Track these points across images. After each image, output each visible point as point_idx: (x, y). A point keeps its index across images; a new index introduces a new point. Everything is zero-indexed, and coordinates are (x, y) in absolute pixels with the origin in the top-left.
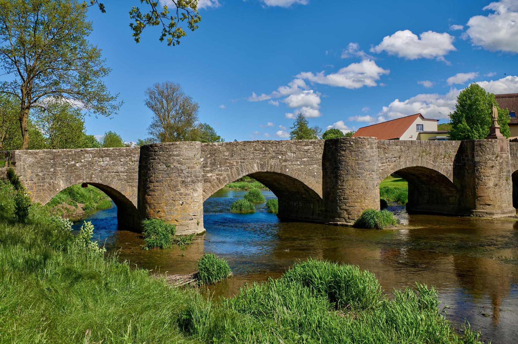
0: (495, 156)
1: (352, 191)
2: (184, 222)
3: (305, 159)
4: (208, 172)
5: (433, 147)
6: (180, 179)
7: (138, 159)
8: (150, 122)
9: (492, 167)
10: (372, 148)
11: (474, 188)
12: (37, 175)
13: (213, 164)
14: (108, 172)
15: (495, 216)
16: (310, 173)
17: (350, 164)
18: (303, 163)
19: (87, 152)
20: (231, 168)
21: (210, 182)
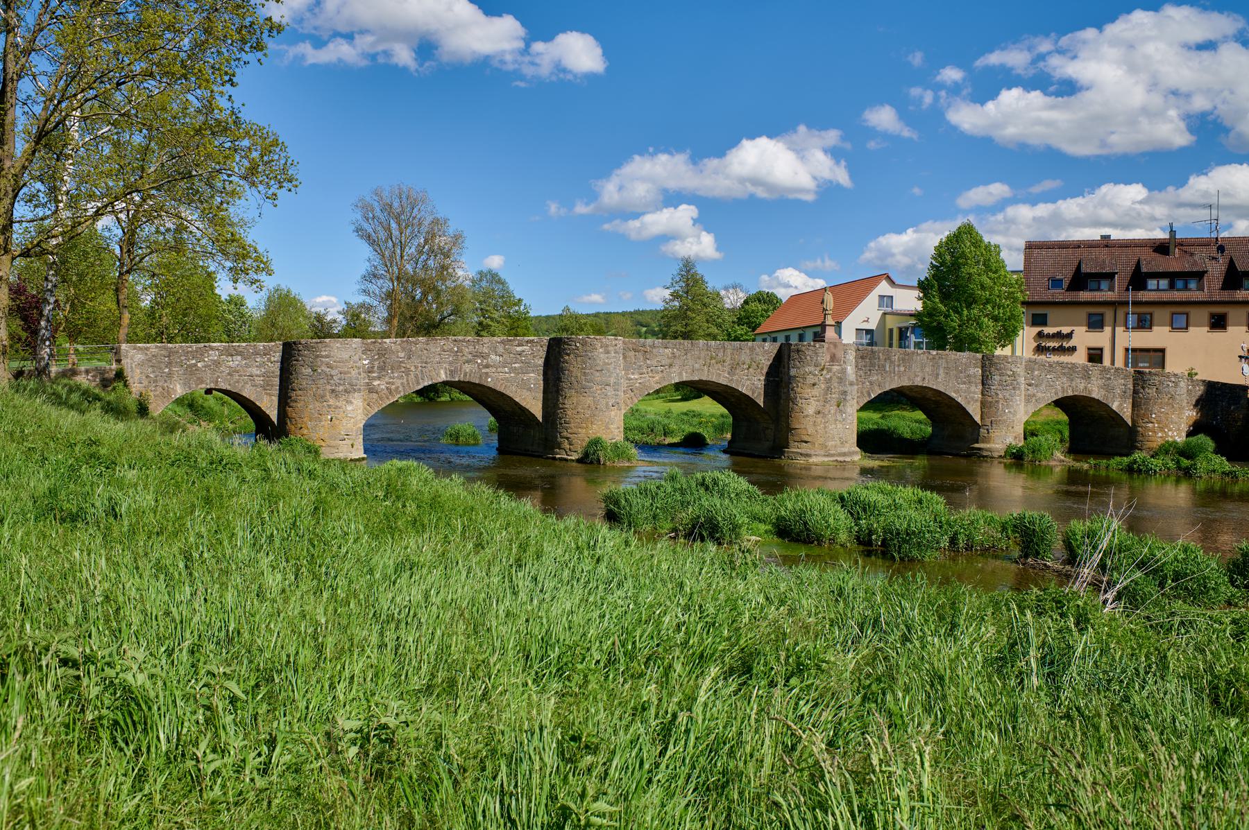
0: (818, 369)
1: (575, 412)
2: (333, 443)
3: (516, 365)
4: (374, 378)
5: (729, 352)
6: (329, 387)
7: (280, 359)
8: (363, 268)
9: (814, 385)
11: (787, 415)
12: (147, 377)
13: (382, 368)
14: (240, 376)
15: (813, 460)
16: (524, 385)
17: (574, 374)
19: (212, 349)
20: (407, 375)
21: (377, 392)
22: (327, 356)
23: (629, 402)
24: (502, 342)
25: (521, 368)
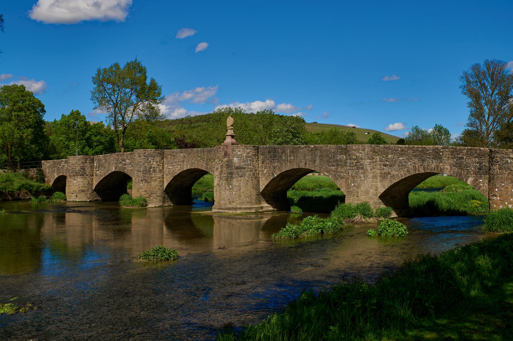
10: (140, 157)
13: (99, 167)
20: (105, 169)
22: (69, 163)
23: (168, 180)
24: (130, 154)
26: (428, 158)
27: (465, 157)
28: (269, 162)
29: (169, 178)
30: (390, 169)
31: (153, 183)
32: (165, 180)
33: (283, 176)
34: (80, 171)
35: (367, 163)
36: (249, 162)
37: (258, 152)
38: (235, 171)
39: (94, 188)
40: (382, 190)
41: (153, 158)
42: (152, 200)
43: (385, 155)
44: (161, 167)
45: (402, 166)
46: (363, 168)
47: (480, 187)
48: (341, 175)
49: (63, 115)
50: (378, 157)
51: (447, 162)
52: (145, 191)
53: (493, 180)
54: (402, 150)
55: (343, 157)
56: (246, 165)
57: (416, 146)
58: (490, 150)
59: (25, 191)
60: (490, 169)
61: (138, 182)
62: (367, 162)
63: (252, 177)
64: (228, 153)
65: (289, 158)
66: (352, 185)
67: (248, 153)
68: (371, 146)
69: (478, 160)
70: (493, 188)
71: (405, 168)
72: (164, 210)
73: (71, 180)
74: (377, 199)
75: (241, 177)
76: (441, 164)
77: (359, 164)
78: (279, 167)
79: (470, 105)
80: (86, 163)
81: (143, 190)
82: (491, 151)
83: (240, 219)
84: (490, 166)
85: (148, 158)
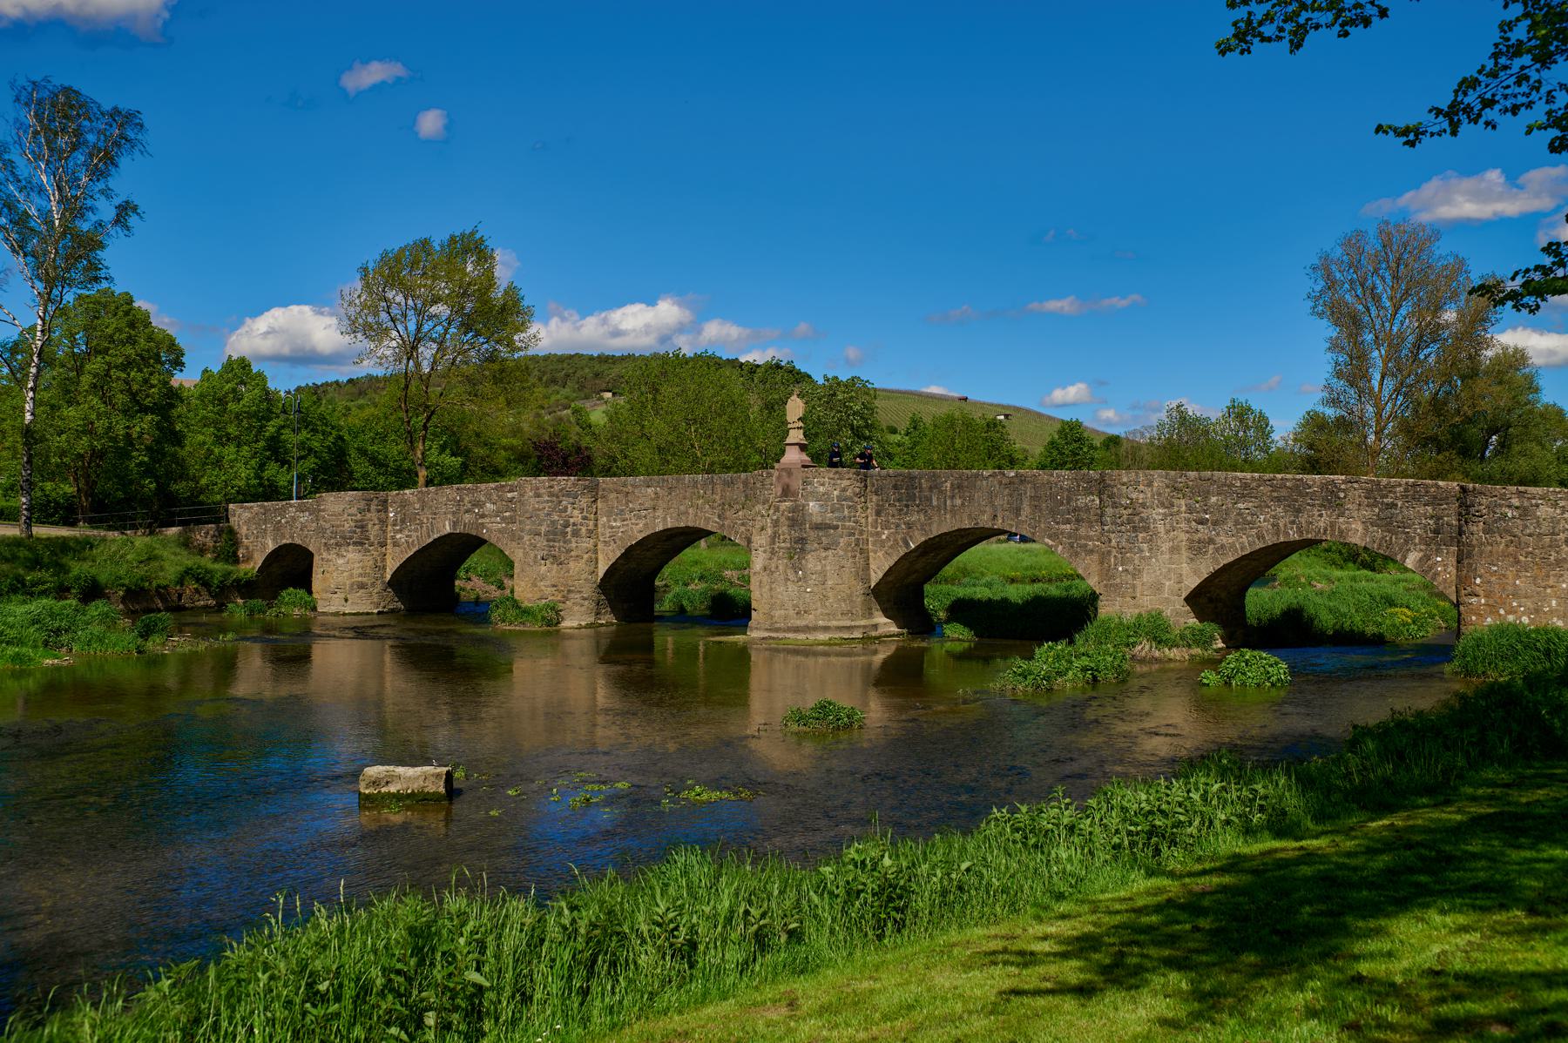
3: (507, 514)
6: (323, 541)
10: (538, 496)
13: (403, 521)
18: (503, 519)
19: (291, 506)
22: (324, 510)
24: (496, 489)
25: (511, 517)
26: (1308, 504)
27: (1400, 504)
28: (896, 513)
29: (613, 551)
30: (1214, 530)
31: (572, 565)
32: (601, 557)
33: (928, 547)
34: (355, 532)
35: (1157, 517)
36: (846, 512)
37: (866, 486)
38: (813, 534)
39: (388, 577)
40: (1193, 582)
41: (571, 500)
42: (571, 609)
43: (1200, 496)
44: (591, 523)
45: (1243, 523)
46: (1146, 529)
47: (1437, 574)
48: (1086, 545)
49: (205, 371)
50: (1183, 502)
51: (1355, 514)
52: (554, 586)
53: (1470, 555)
54: (1245, 486)
55: (1094, 500)
56: (839, 519)
57: (1279, 476)
58: (1462, 487)
59: (195, 586)
60: (1461, 533)
61: (535, 562)
62: (1157, 513)
63: (853, 550)
64: (792, 489)
65: (948, 502)
66: (1120, 569)
67: (844, 490)
68: (1167, 474)
69: (1431, 511)
70: (1470, 577)
71: (1251, 528)
72: (598, 635)
73: (330, 557)
74: (1180, 605)
75: (826, 549)
76: (1341, 520)
77: (1136, 518)
78: (922, 525)
79: (1335, 346)
80: (369, 511)
81: (548, 583)
82: (1464, 490)
83: (826, 654)
84: (1460, 527)
85: (561, 498)
